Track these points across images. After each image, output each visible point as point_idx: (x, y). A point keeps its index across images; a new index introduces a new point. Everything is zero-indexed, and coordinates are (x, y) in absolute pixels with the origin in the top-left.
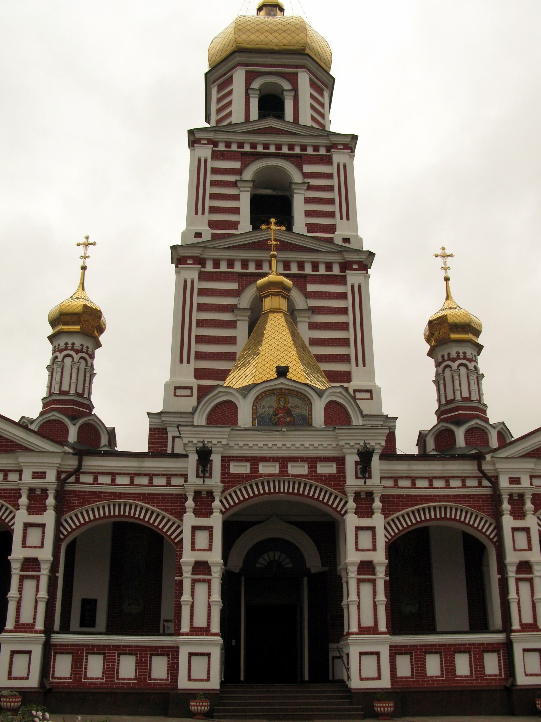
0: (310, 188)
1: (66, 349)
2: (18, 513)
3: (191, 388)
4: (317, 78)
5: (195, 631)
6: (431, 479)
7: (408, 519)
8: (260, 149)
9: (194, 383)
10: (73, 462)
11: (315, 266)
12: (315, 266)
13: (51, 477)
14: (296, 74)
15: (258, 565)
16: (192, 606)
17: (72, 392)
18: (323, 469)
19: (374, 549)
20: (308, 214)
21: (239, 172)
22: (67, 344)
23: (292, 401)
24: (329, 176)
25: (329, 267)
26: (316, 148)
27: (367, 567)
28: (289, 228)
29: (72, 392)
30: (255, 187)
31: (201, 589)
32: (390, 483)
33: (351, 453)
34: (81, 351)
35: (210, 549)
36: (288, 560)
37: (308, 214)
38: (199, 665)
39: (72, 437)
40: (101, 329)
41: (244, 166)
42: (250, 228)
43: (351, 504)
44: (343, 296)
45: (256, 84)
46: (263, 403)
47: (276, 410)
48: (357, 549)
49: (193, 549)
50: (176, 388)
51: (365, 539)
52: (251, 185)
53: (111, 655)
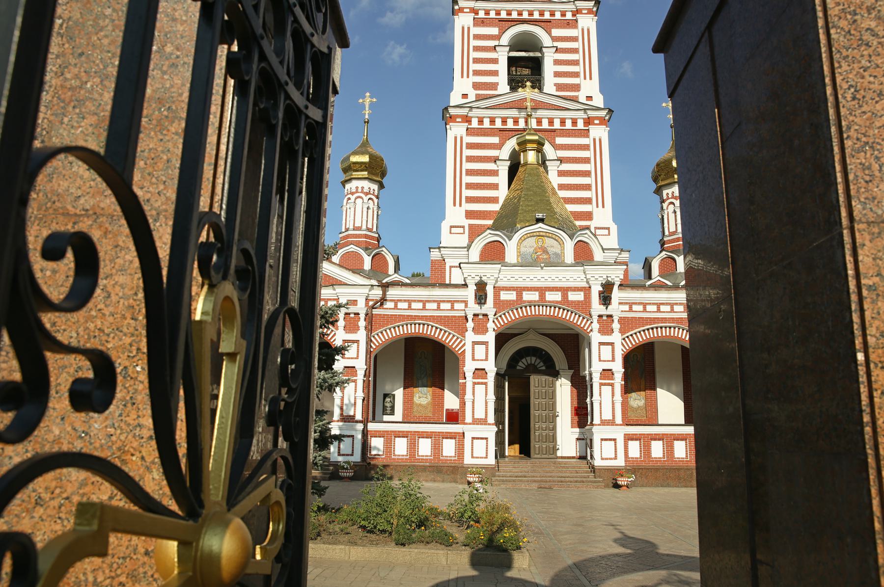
0: (557, 50)
1: (357, 192)
2: (337, 332)
3: (463, 227)
5: (476, 422)
6: (659, 305)
7: (640, 338)
8: (515, 15)
9: (466, 223)
10: (377, 293)
11: (563, 122)
12: (563, 122)
13: (361, 303)
15: (518, 368)
16: (473, 403)
17: (364, 227)
18: (573, 297)
19: (613, 360)
20: (557, 74)
22: (357, 188)
23: (549, 242)
24: (574, 39)
25: (574, 122)
26: (563, 14)
27: (607, 373)
28: (540, 89)
29: (364, 227)
30: (510, 50)
31: (480, 389)
32: (627, 308)
33: (596, 284)
34: (369, 193)
35: (486, 359)
36: (542, 364)
37: (557, 74)
38: (480, 445)
39: (367, 266)
40: (383, 174)
41: (502, 32)
42: (507, 89)
43: (596, 326)
44: (586, 147)
46: (525, 243)
47: (535, 249)
48: (600, 360)
49: (473, 359)
50: (451, 227)
51: (606, 351)
52: (508, 48)
53: (413, 439)
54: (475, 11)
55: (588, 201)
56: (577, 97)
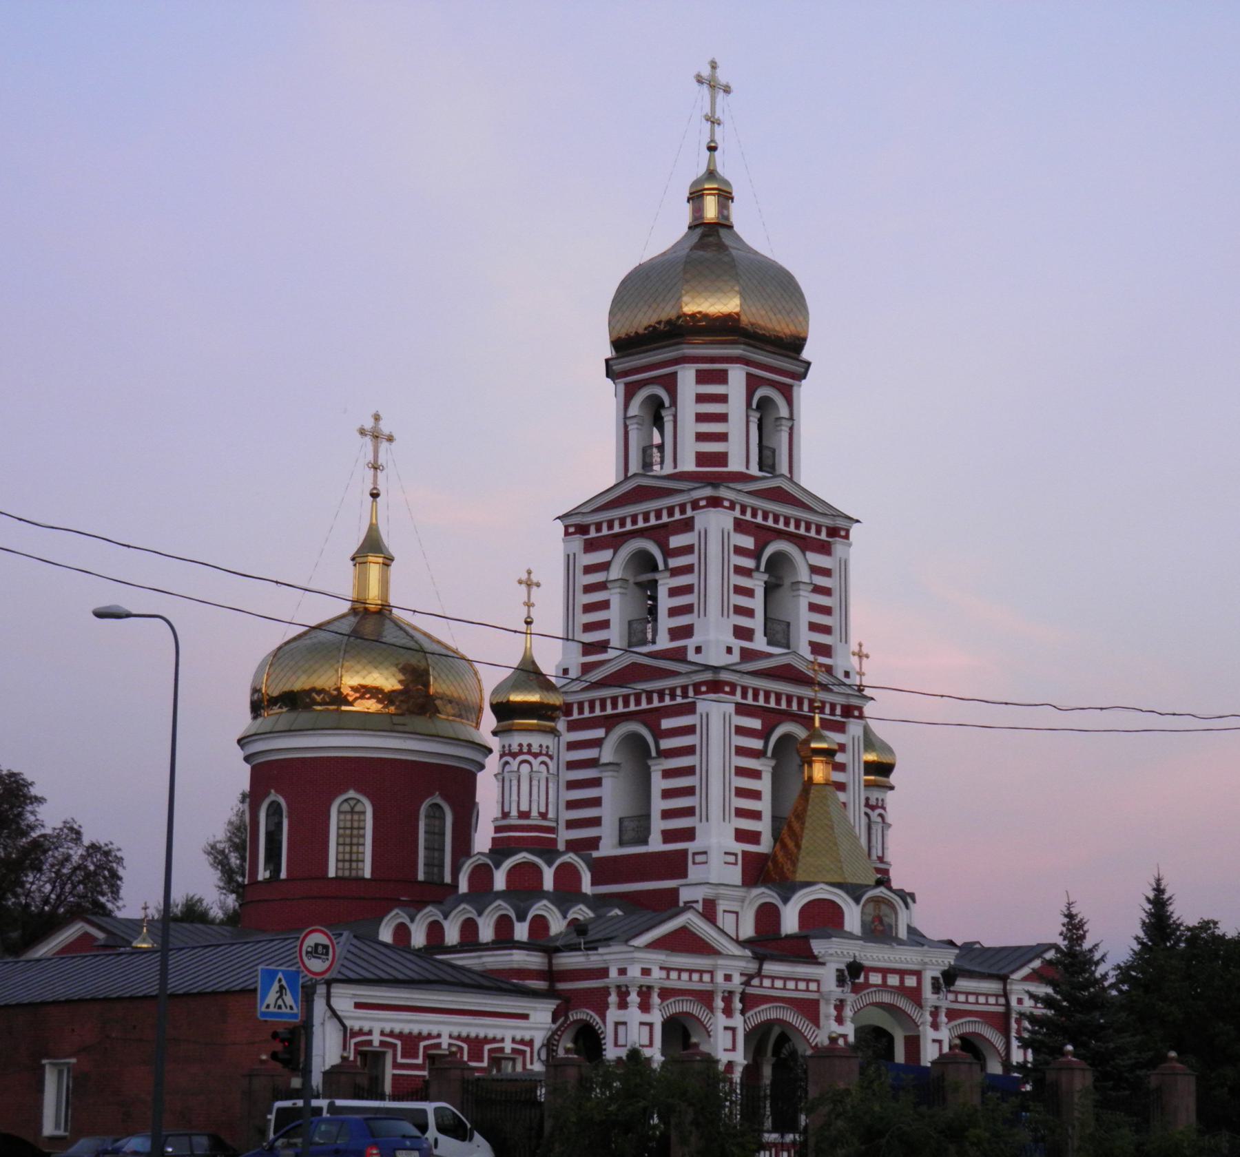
0: (676, 572)
4: (713, 360)
8: (629, 527)
14: (675, 374)
20: (673, 612)
21: (605, 566)
44: (690, 730)
45: (634, 409)
54: (582, 529)
55: (690, 812)
56: (685, 648)
